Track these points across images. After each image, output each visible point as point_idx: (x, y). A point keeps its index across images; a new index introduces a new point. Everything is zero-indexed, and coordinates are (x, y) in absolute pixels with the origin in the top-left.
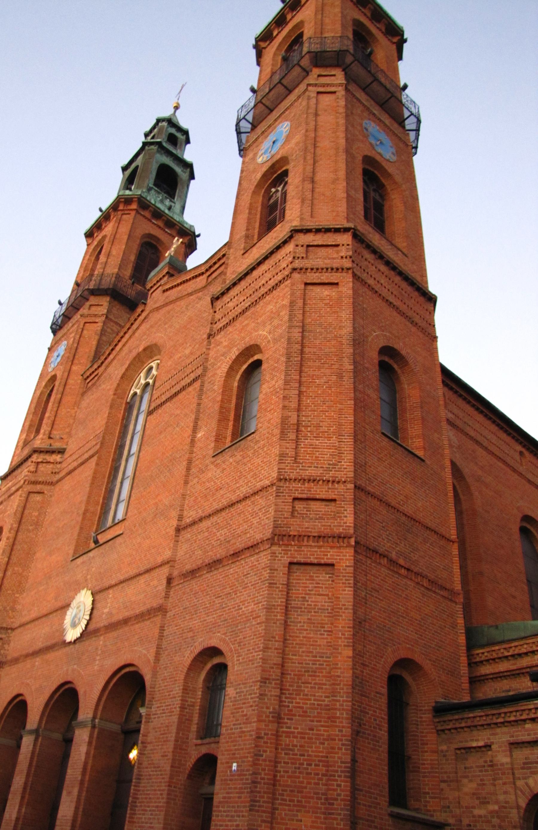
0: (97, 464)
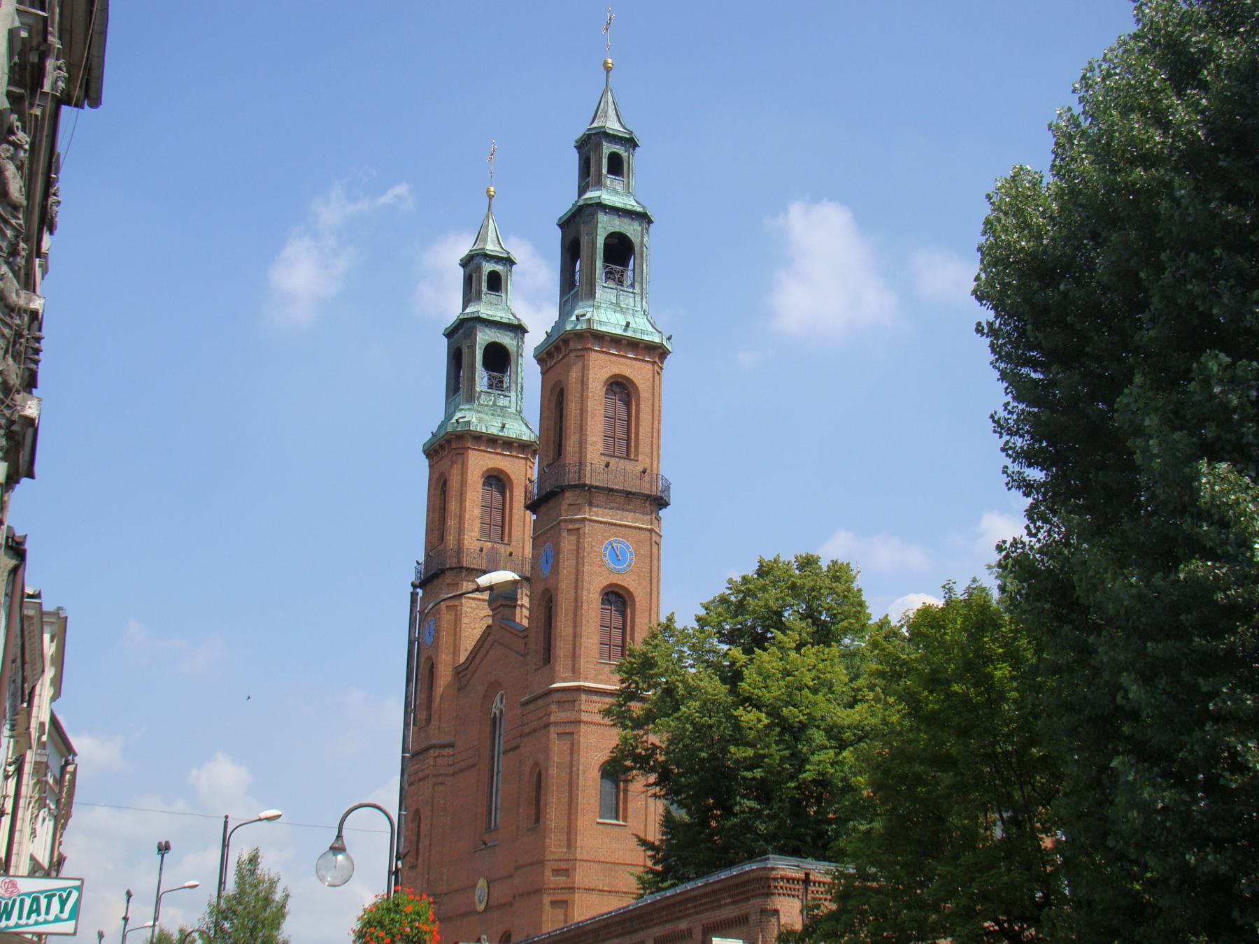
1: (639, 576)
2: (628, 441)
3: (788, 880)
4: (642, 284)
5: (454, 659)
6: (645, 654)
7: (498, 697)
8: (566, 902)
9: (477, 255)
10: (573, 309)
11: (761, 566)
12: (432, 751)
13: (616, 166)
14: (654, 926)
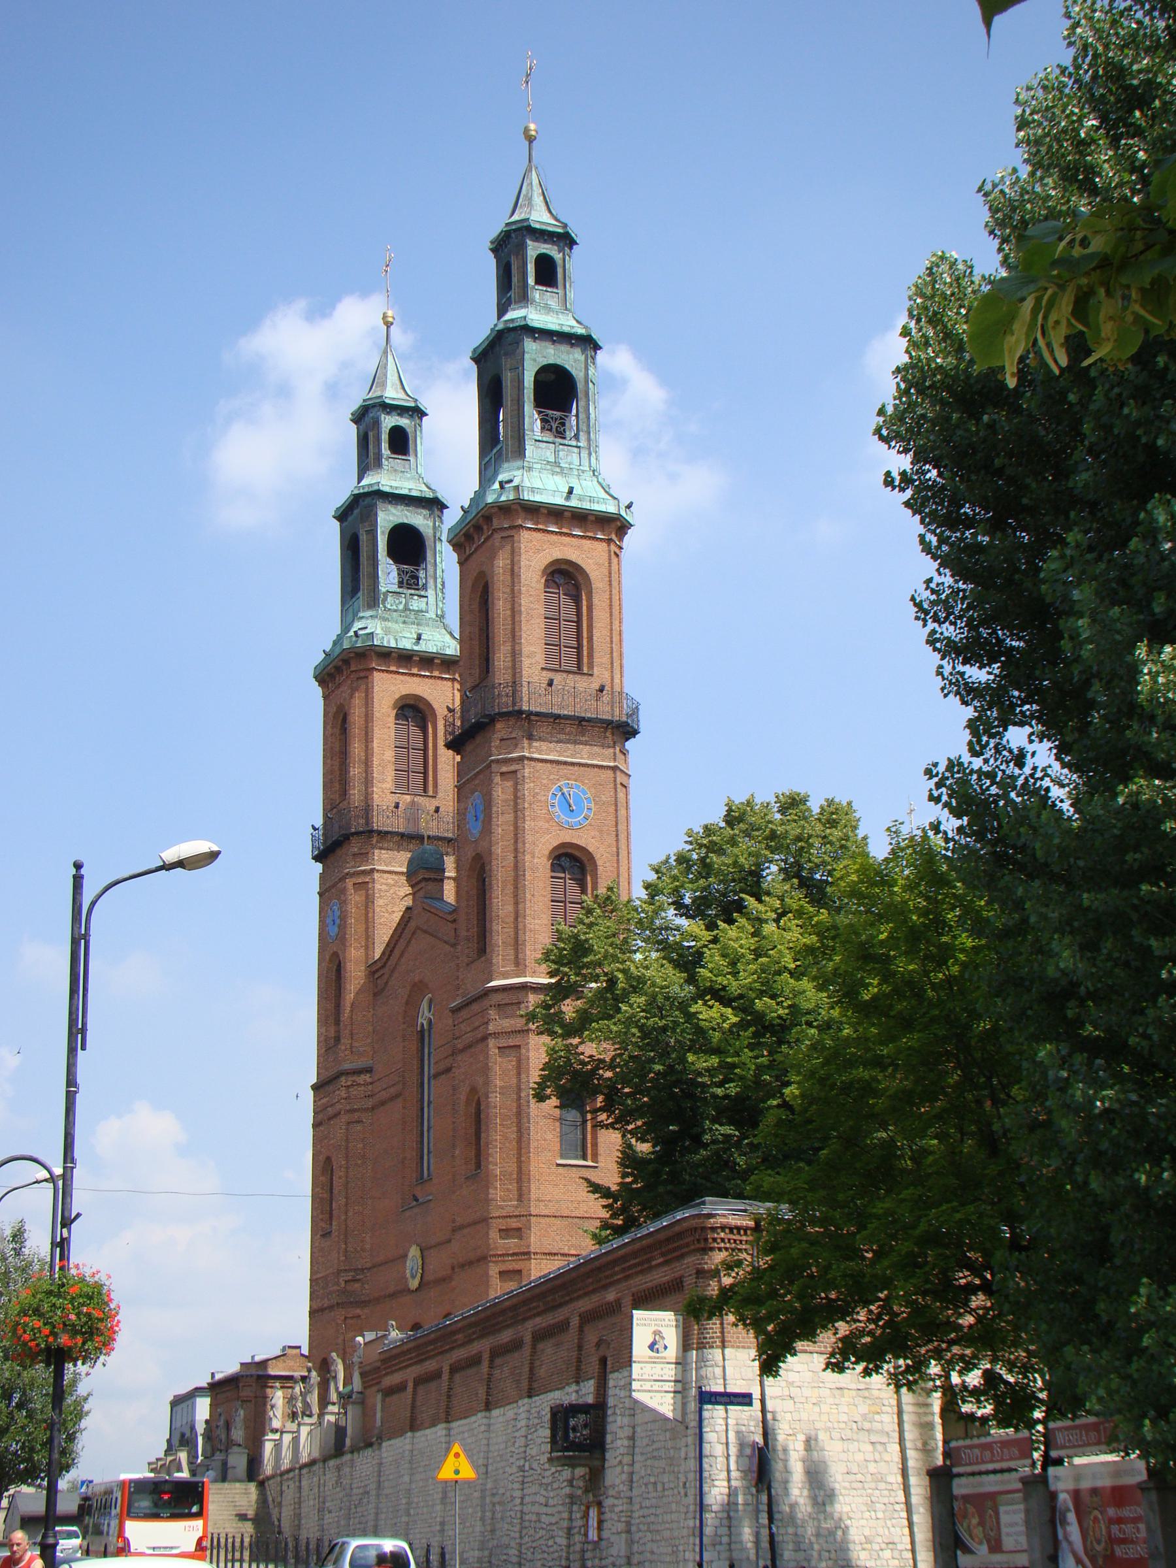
0: (404, 1108)
1: (601, 831)
2: (579, 648)
3: (731, 1230)
4: (589, 433)
5: (367, 955)
6: (576, 936)
7: (425, 1004)
8: (519, 1272)
9: (374, 406)
10: (496, 474)
11: (730, 810)
12: (343, 1079)
13: (547, 273)
14: (579, 1298)
